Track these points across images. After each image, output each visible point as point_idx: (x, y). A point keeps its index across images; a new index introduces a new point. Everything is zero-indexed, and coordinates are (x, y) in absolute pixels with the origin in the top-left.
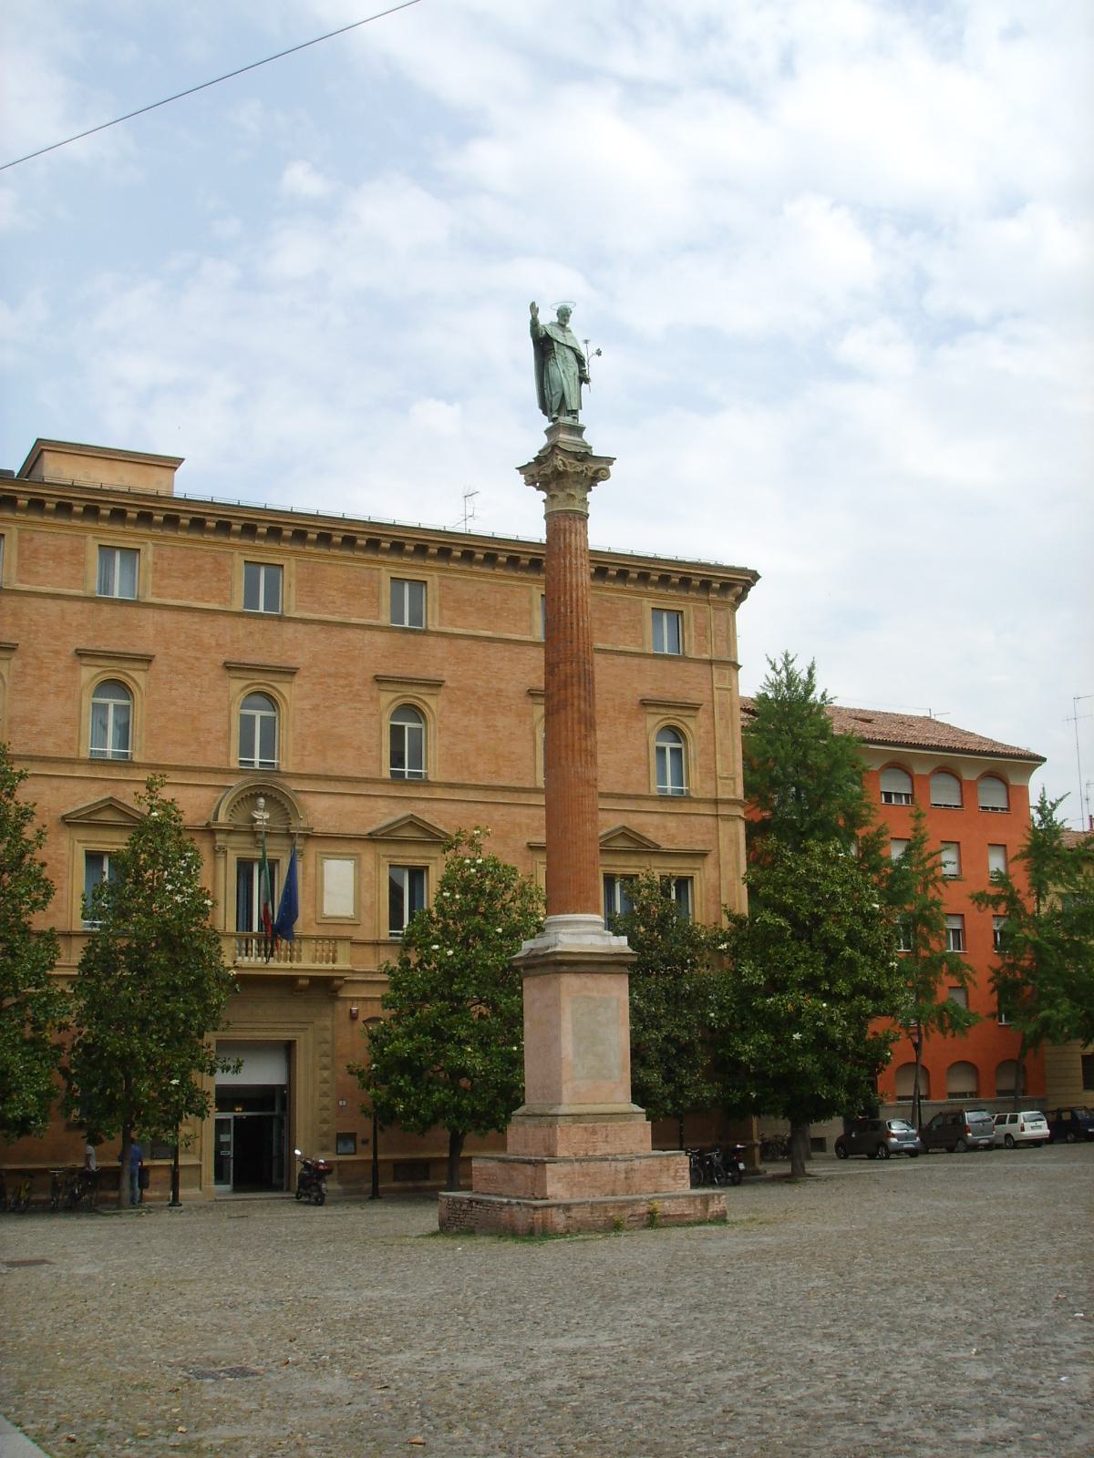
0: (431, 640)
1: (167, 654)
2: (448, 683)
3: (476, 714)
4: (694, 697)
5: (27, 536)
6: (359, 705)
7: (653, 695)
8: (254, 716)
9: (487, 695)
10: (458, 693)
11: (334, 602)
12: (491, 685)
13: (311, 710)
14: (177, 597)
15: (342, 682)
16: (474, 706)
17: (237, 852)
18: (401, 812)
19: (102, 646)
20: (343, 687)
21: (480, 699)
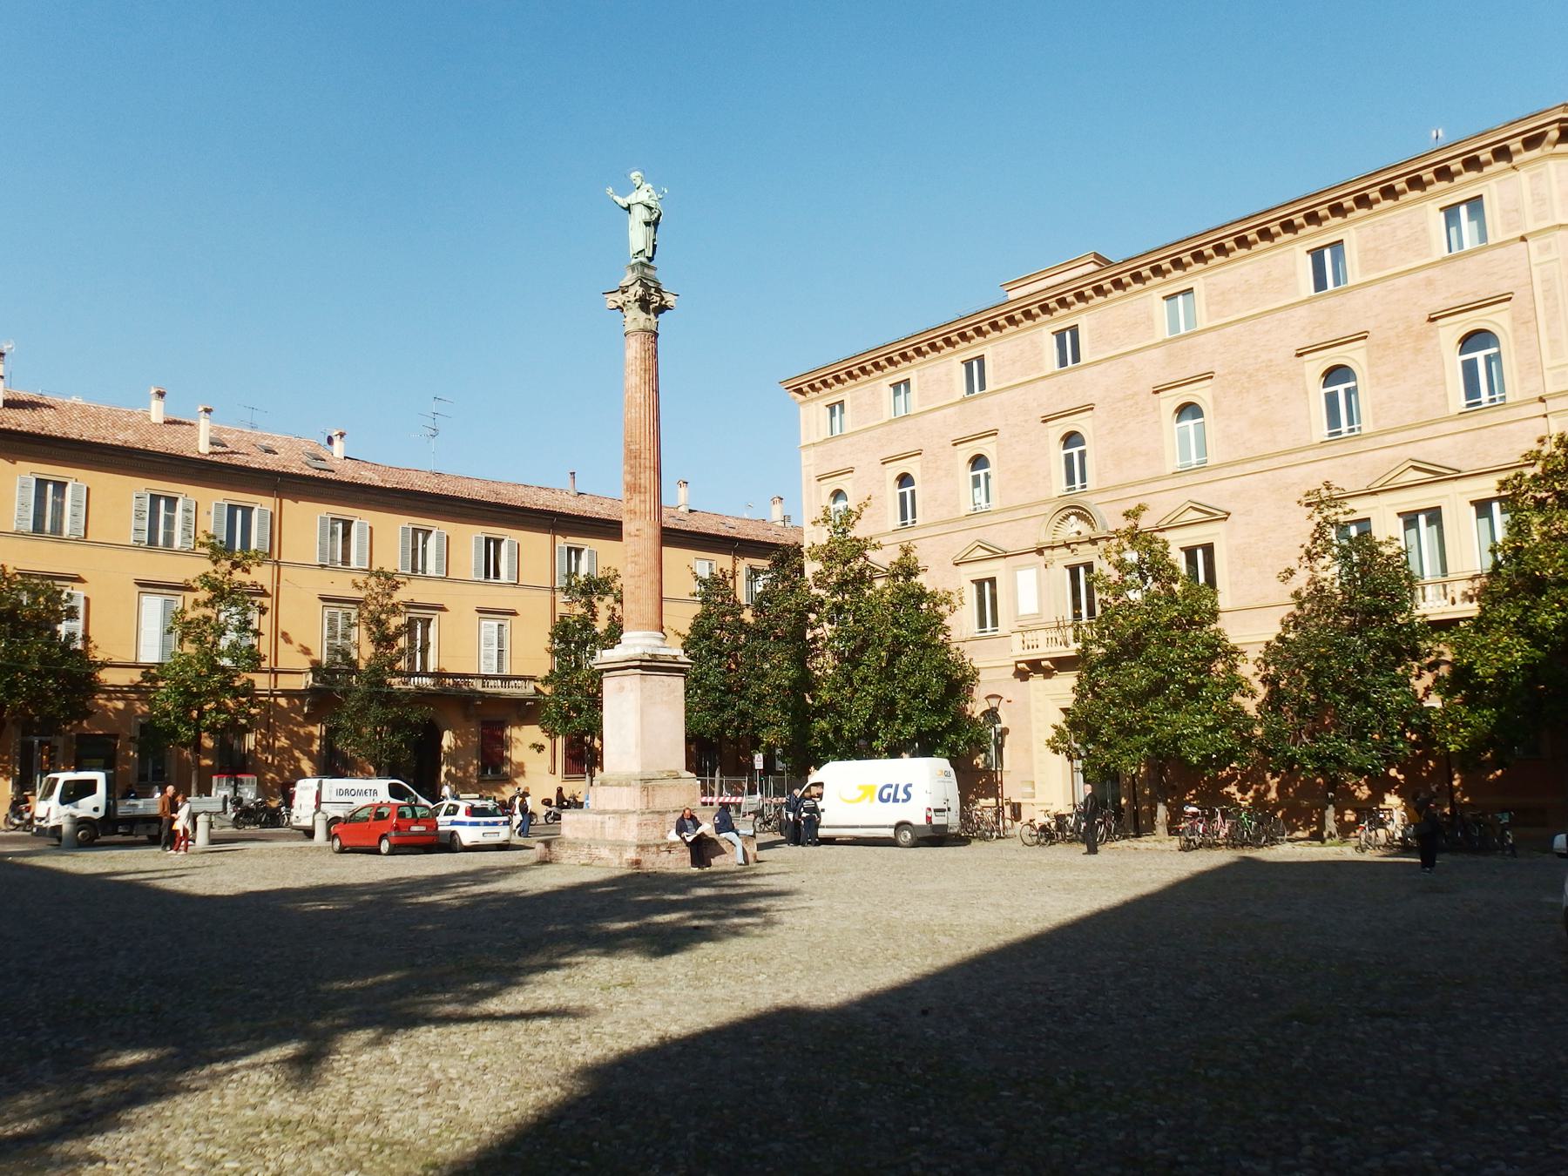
0: (1202, 339)
1: (1007, 425)
2: (1218, 371)
3: (1248, 392)
4: (1504, 288)
5: (921, 374)
6: (1144, 418)
7: (1305, 342)
8: (1476, 359)
9: (1257, 370)
10: (1230, 378)
11: (1118, 338)
12: (1260, 360)
13: (1108, 434)
14: (1009, 380)
15: (1129, 403)
16: (1246, 385)
17: (1395, 508)
18: (1181, 498)
19: (966, 433)
20: (1131, 407)
21: (1250, 376)
